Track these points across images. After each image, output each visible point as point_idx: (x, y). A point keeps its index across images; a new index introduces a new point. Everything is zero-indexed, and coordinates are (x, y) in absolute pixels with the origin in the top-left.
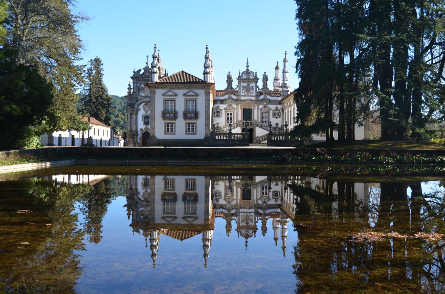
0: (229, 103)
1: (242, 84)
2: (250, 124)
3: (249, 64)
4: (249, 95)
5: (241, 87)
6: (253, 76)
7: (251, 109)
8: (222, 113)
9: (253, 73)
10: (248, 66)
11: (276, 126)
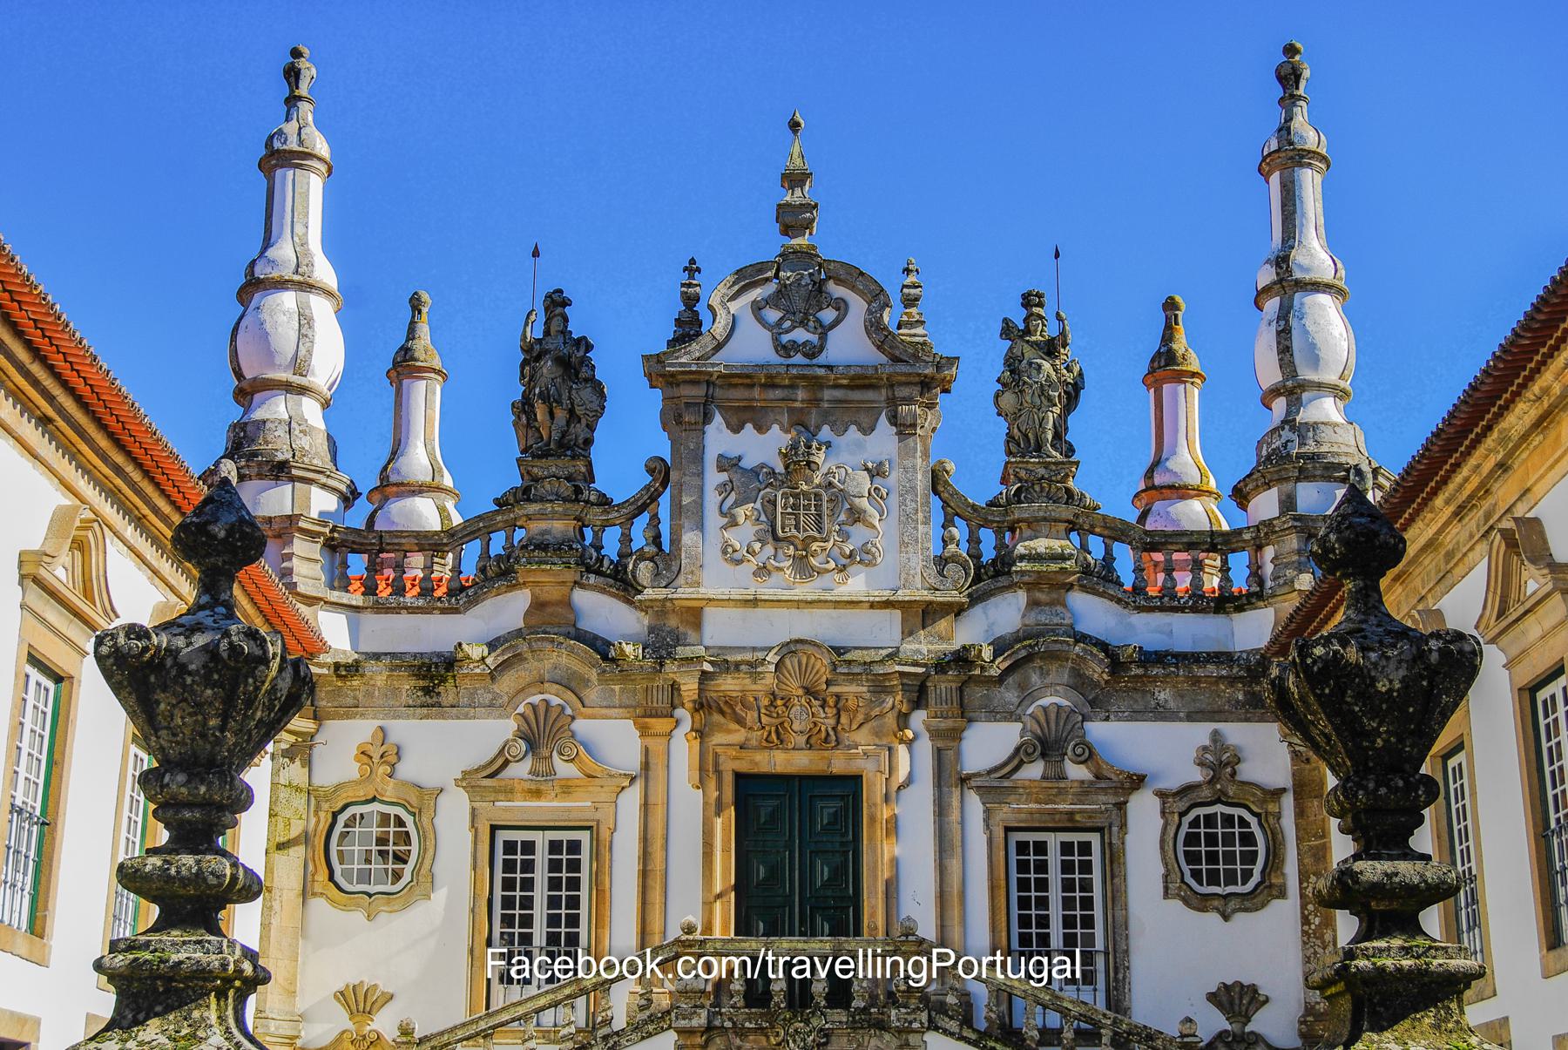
1: (718, 438)
5: (714, 478)
6: (874, 327)
7: (855, 780)
8: (429, 837)
9: (876, 296)
11: (1212, 1022)
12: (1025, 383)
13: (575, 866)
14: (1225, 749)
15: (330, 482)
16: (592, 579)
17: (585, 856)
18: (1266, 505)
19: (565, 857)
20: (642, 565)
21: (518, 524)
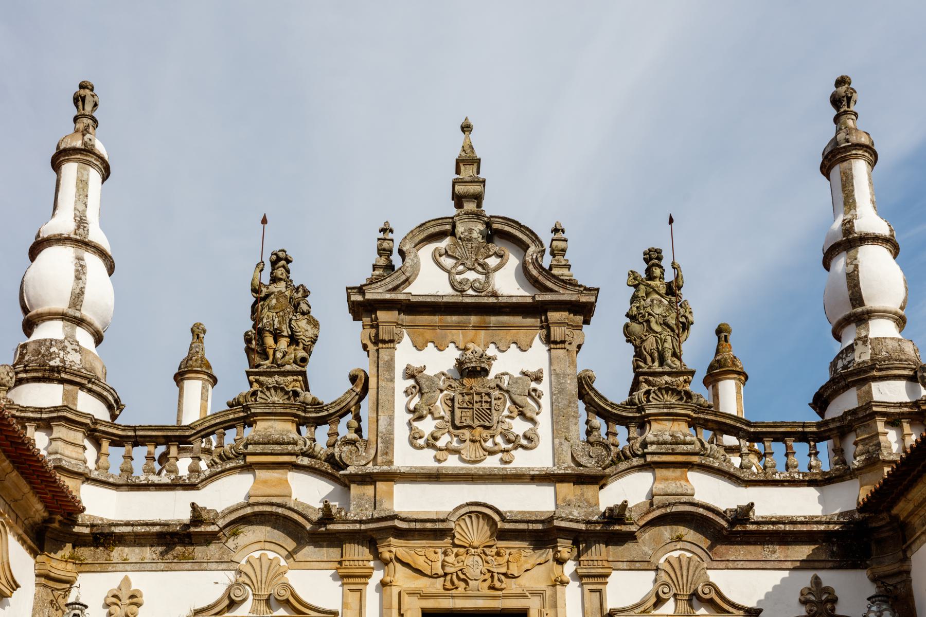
4: (492, 463)
12: (650, 314)
14: (829, 591)
15: (95, 388)
16: (306, 461)
18: (848, 401)
20: (345, 449)
21: (247, 421)
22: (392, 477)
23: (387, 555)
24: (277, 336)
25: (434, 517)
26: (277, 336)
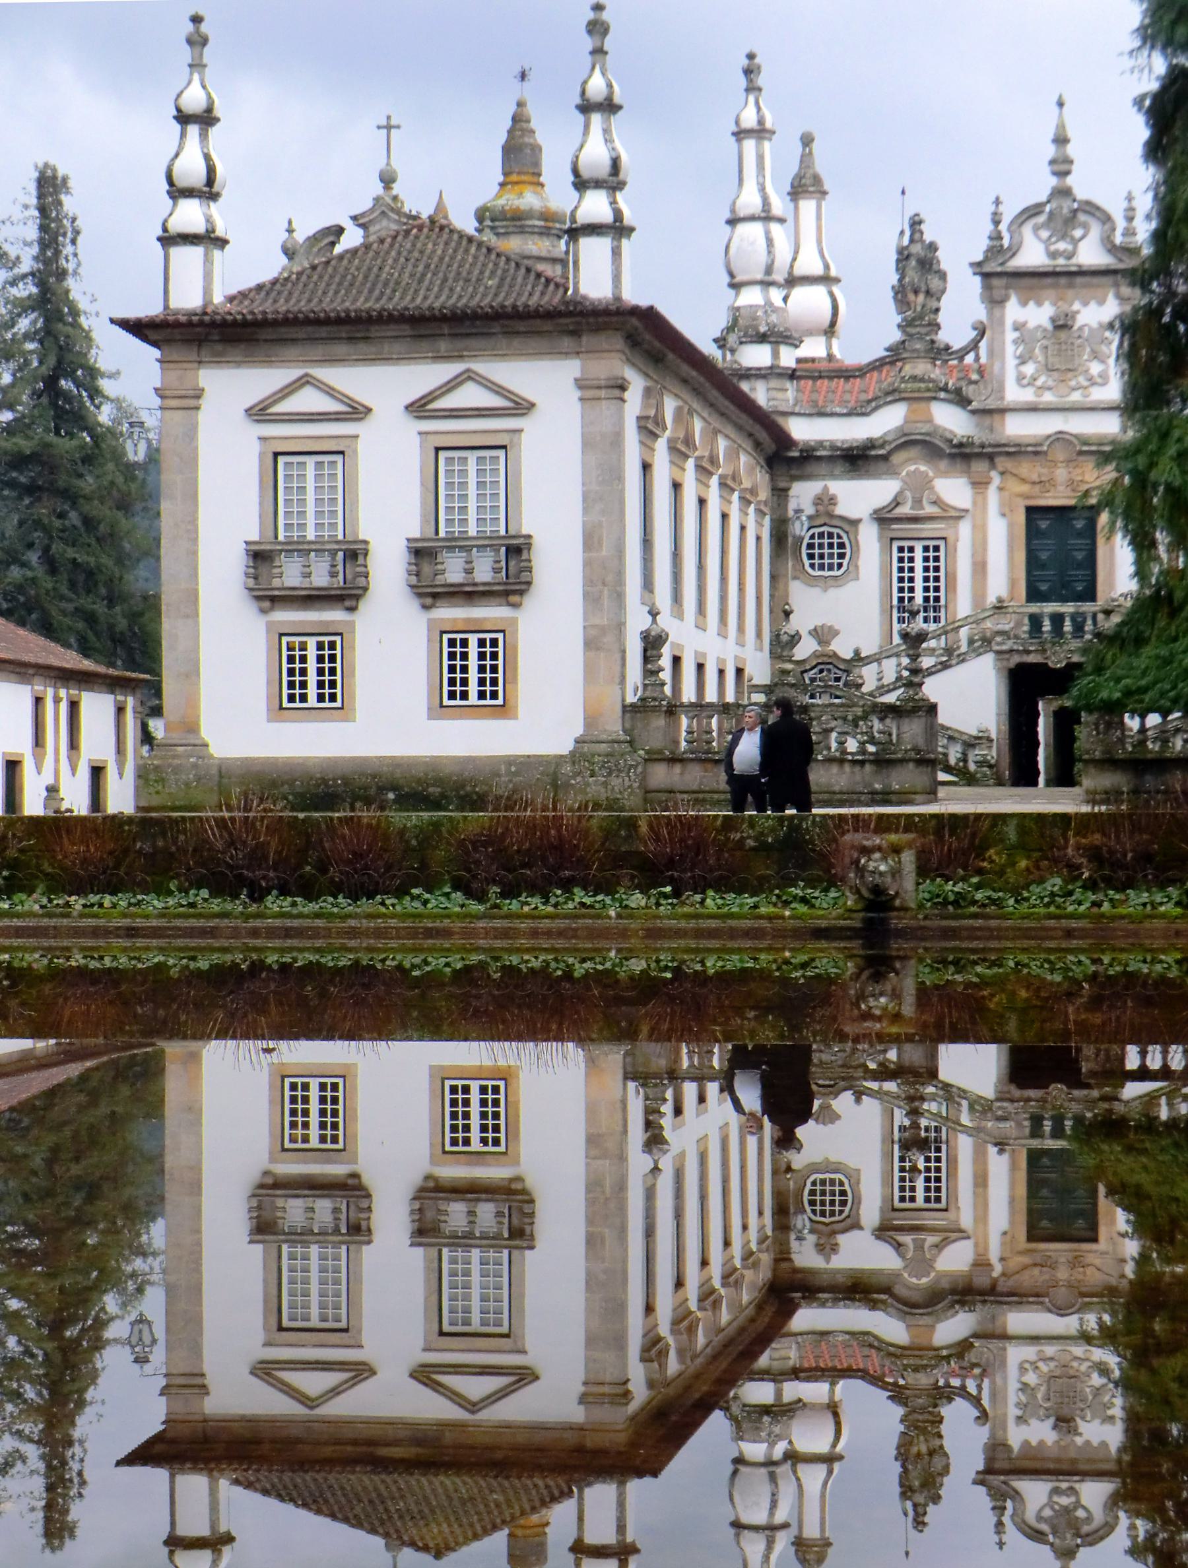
0: (914, 466)
1: (1014, 311)
2: (1068, 627)
3: (1071, 150)
4: (1076, 397)
5: (1010, 335)
9: (1106, 219)
10: (1061, 166)
13: (937, 559)
16: (942, 395)
17: (942, 554)
19: (933, 553)
20: (972, 387)
22: (1003, 411)
23: (1001, 469)
24: (916, 292)
25: (1032, 441)
26: (916, 292)
